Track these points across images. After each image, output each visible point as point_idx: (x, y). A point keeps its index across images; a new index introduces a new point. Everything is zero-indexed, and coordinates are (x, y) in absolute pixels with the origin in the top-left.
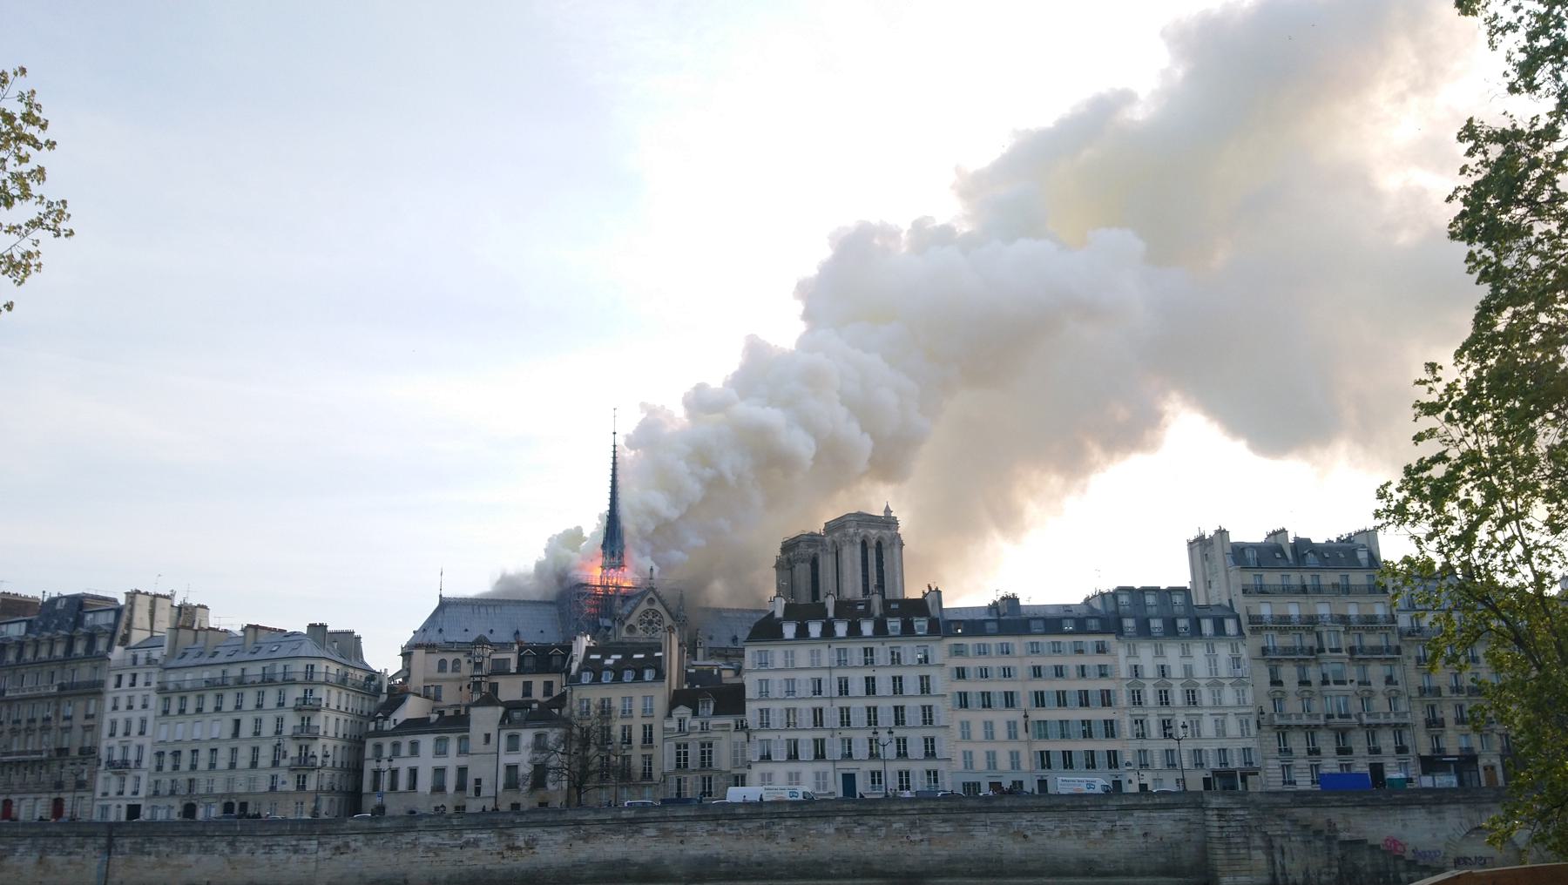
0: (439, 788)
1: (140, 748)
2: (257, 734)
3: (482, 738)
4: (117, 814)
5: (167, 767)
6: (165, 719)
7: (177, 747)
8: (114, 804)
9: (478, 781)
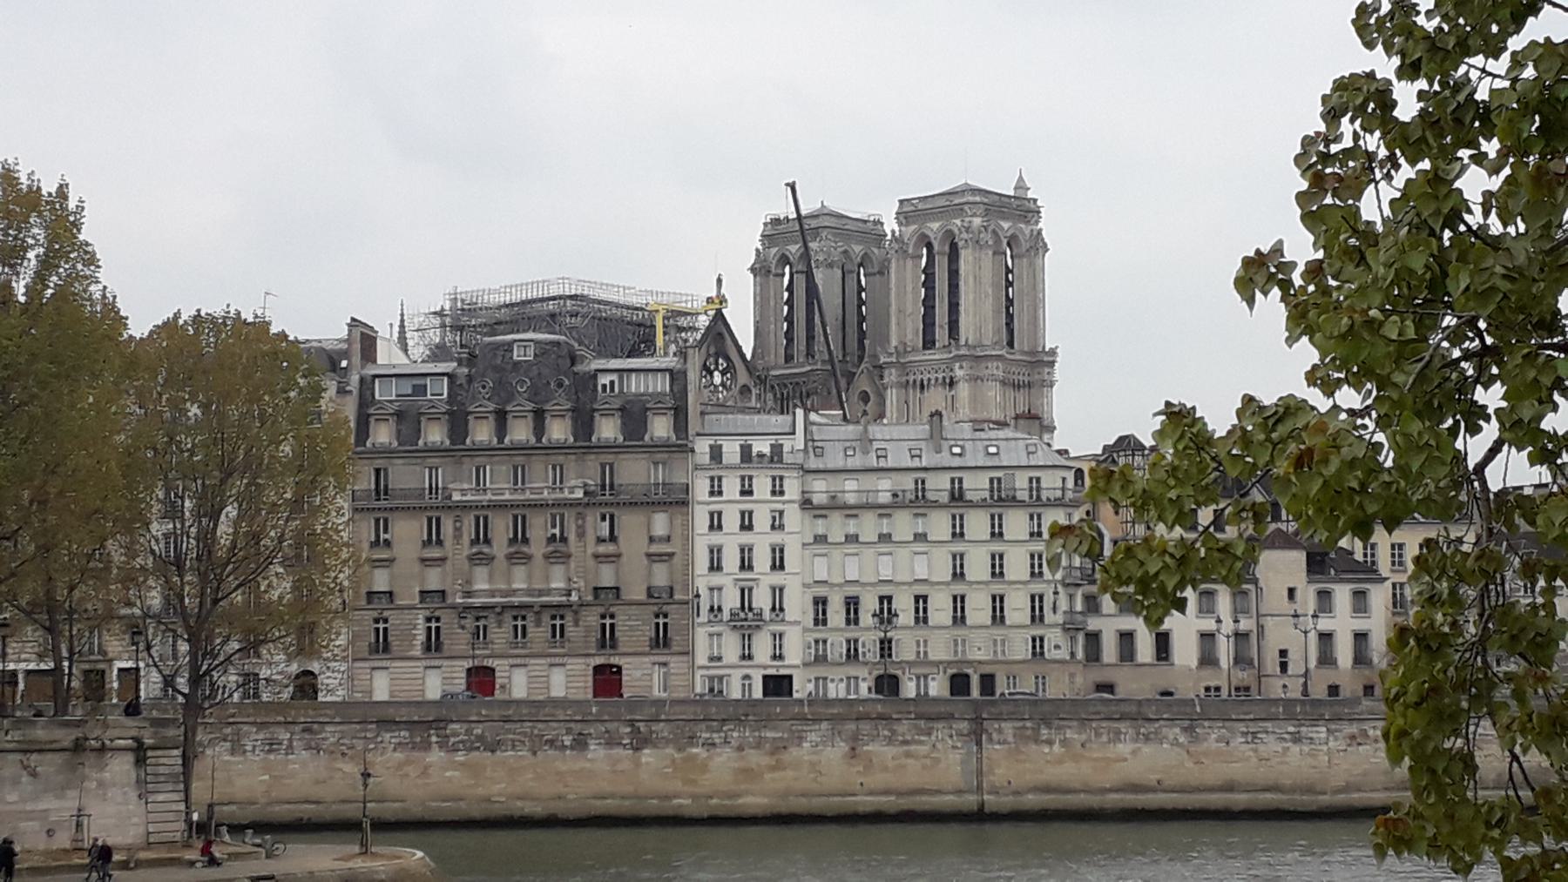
0: (1208, 659)
1: (778, 592)
2: (997, 572)
3: (1285, 593)
4: (744, 684)
5: (836, 616)
6: (821, 549)
7: (852, 591)
8: (736, 675)
9: (1283, 653)
